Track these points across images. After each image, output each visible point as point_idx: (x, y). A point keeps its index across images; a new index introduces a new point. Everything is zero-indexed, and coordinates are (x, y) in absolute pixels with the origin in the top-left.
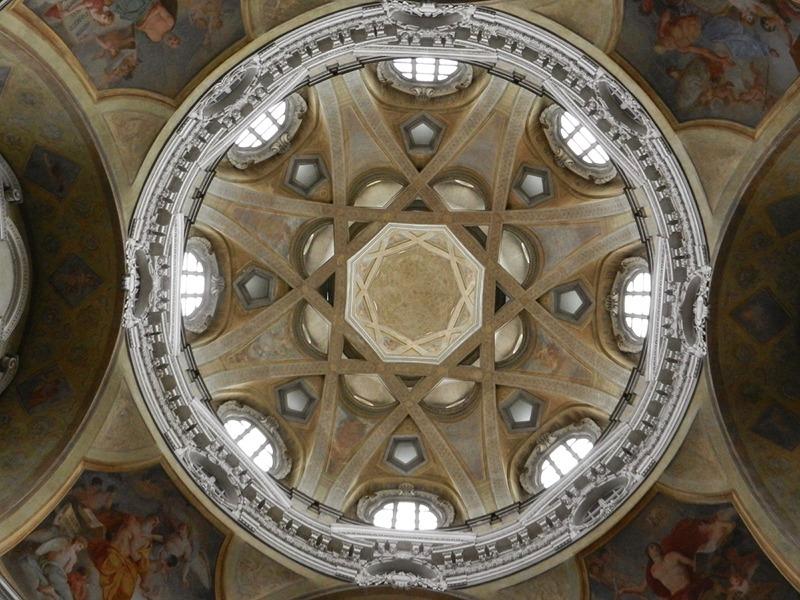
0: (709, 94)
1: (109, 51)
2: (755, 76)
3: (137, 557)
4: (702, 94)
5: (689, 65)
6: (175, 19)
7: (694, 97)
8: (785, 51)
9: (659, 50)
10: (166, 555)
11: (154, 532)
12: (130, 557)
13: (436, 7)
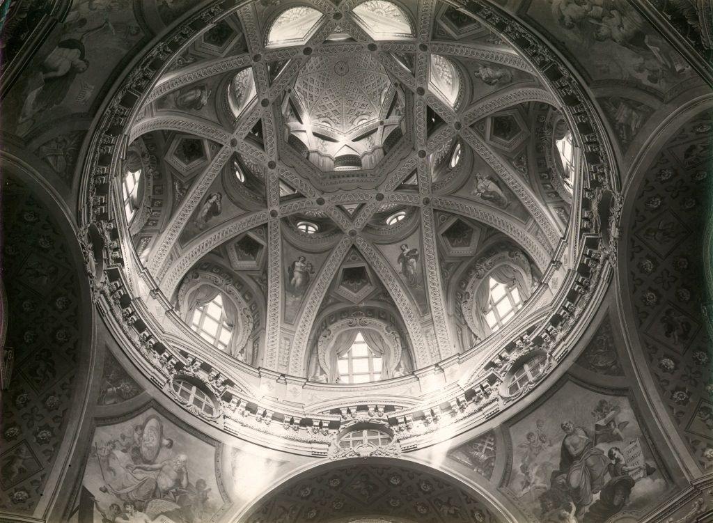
0: (136, 436)
1: (615, 426)
2: (110, 466)
3: (614, 12)
4: (141, 435)
5: (158, 454)
6: (564, 441)
7: (146, 430)
8: (98, 495)
9: (183, 457)
10: (586, 7)
11: (599, 27)
12: (622, 15)
13: (359, 455)
